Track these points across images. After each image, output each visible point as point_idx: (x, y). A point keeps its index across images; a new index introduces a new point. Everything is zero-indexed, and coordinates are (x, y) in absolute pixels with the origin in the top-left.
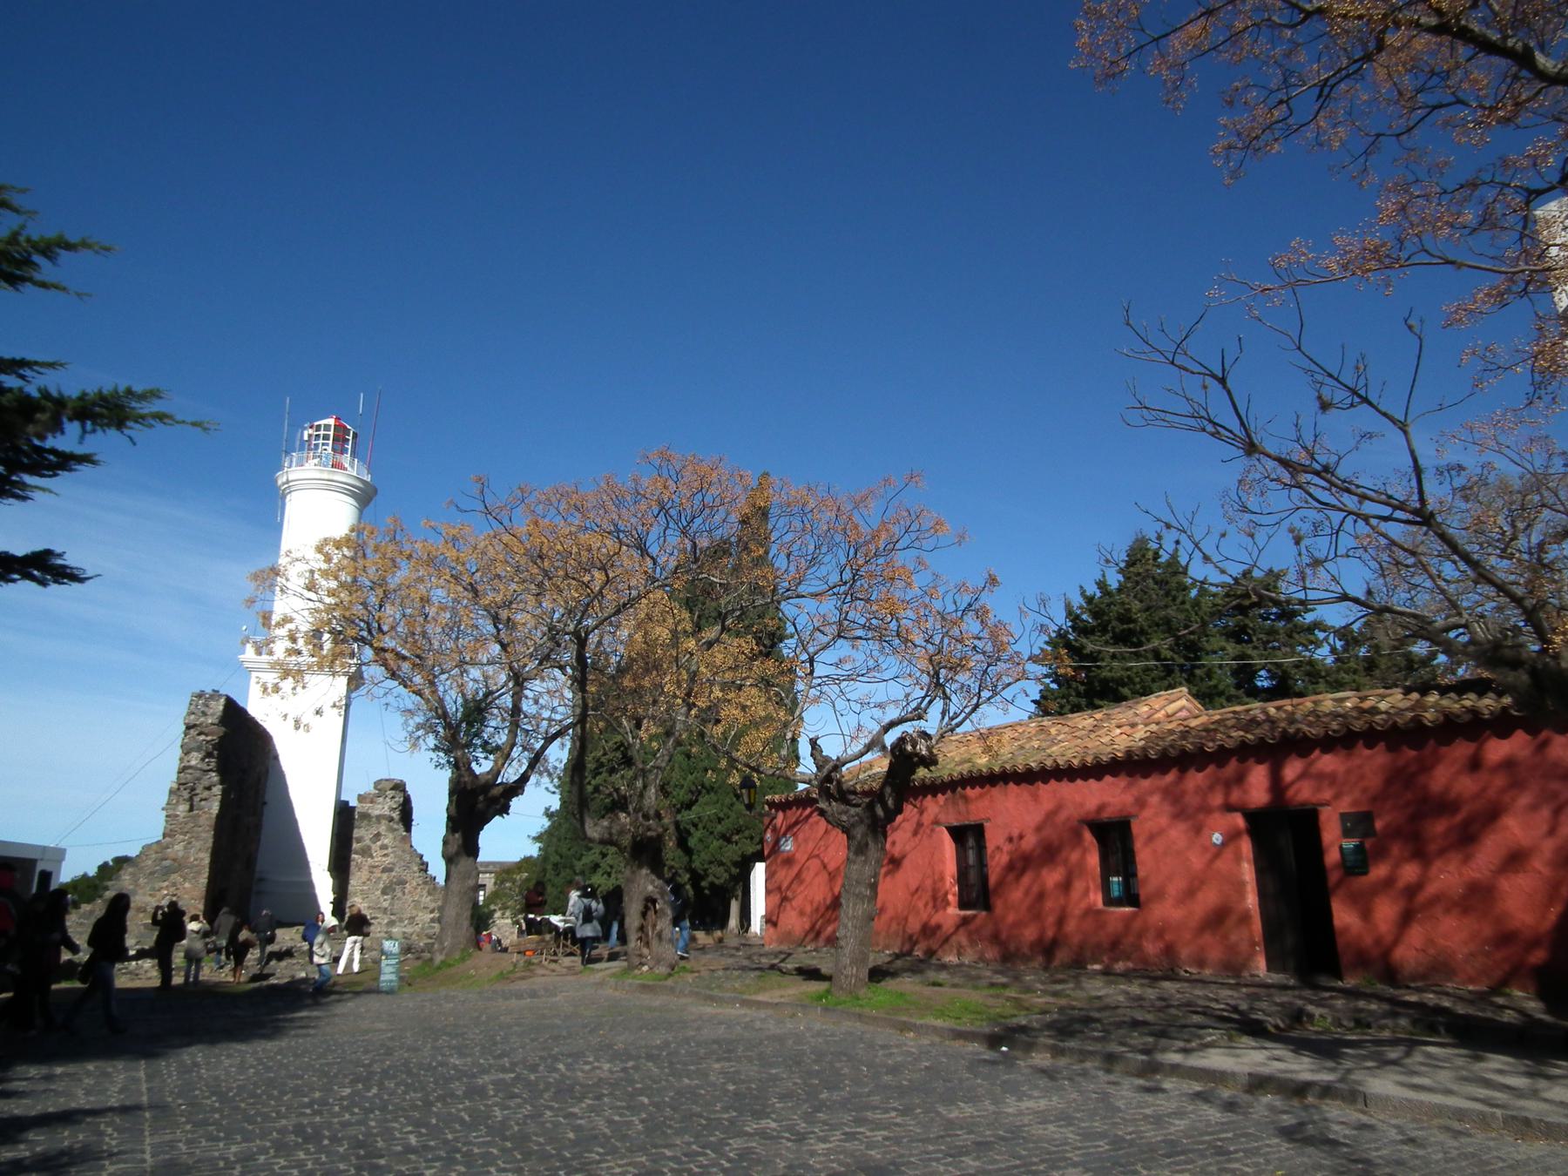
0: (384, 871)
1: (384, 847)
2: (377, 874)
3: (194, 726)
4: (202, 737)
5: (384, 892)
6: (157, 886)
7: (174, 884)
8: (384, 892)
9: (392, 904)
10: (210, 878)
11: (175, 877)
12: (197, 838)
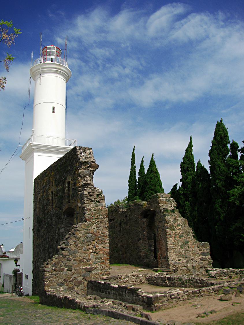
0: (180, 237)
1: (178, 225)
3: (85, 162)
4: (90, 169)
5: (181, 248)
7: (94, 246)
8: (181, 248)
9: (185, 253)
12: (101, 222)
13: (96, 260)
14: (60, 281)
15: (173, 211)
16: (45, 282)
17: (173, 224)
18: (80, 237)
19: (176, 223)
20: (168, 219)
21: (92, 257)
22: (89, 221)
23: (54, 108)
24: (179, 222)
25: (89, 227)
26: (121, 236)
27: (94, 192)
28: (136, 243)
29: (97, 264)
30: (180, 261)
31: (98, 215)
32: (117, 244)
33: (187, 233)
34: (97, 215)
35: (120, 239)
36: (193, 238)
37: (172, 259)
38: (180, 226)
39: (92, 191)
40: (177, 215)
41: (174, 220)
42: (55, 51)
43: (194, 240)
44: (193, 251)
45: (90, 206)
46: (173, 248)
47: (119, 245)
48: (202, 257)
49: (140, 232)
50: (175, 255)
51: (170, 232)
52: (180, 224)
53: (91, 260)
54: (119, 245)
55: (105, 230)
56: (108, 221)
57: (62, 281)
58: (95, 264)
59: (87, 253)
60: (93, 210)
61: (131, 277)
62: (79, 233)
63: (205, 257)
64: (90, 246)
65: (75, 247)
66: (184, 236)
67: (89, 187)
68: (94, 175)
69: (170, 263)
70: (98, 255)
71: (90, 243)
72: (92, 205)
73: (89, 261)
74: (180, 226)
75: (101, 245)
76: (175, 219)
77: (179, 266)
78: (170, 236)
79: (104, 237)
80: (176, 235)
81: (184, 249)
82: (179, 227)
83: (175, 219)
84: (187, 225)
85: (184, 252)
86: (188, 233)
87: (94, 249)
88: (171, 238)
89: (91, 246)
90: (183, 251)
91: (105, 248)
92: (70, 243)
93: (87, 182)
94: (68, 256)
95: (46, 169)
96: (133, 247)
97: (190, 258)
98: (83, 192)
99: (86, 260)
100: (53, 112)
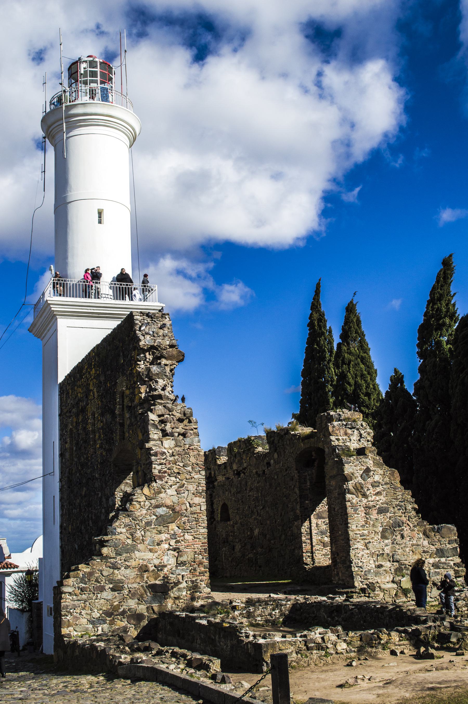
0: (381, 511)
1: (375, 485)
2: (374, 515)
5: (384, 537)
6: (158, 537)
7: (174, 536)
8: (384, 537)
10: (209, 527)
11: (173, 527)
13: (176, 567)
14: (96, 614)
15: (361, 452)
16: (63, 618)
17: (363, 482)
18: (142, 515)
19: (369, 479)
20: (351, 470)
21: (168, 560)
22: (161, 478)
23: (100, 214)
24: (377, 478)
25: (161, 492)
26: (259, 511)
27: (172, 415)
28: (290, 528)
29: (179, 575)
30: (379, 569)
31: (181, 464)
32: (252, 530)
33: (397, 503)
34: (179, 465)
35: (257, 517)
36: (414, 513)
37: (360, 564)
38: (381, 487)
39: (168, 412)
40: (371, 462)
41: (363, 472)
42: (98, 70)
43: (415, 520)
44: (413, 545)
45: (161, 446)
46: (362, 540)
47: (256, 532)
48: (437, 559)
49: (296, 499)
50: (368, 554)
51: (354, 501)
52: (379, 483)
53: (165, 566)
54: (256, 532)
55: (198, 498)
56: (204, 477)
57: (101, 614)
58: (175, 576)
59: (156, 552)
60: (168, 454)
61: (261, 605)
62: (138, 506)
63: (446, 560)
64: (163, 537)
65: (129, 538)
66: (392, 509)
67: (161, 404)
68: (173, 375)
69: (354, 573)
70: (181, 556)
71: (163, 529)
72: (168, 443)
73: (162, 570)
74: (381, 487)
75: (187, 532)
76: (367, 470)
77: (379, 581)
78: (356, 510)
79: (195, 513)
80: (370, 508)
81: (390, 541)
82: (378, 489)
83: (367, 470)
84: (399, 485)
85: (392, 548)
86: (400, 502)
87: (173, 542)
88: (356, 515)
89: (166, 535)
90: (387, 545)
91: (198, 540)
92: (119, 530)
93: (156, 393)
94: (114, 558)
95: (80, 361)
96: (283, 537)
97: (405, 562)
98: (148, 415)
99: (155, 566)
100: (100, 222)
